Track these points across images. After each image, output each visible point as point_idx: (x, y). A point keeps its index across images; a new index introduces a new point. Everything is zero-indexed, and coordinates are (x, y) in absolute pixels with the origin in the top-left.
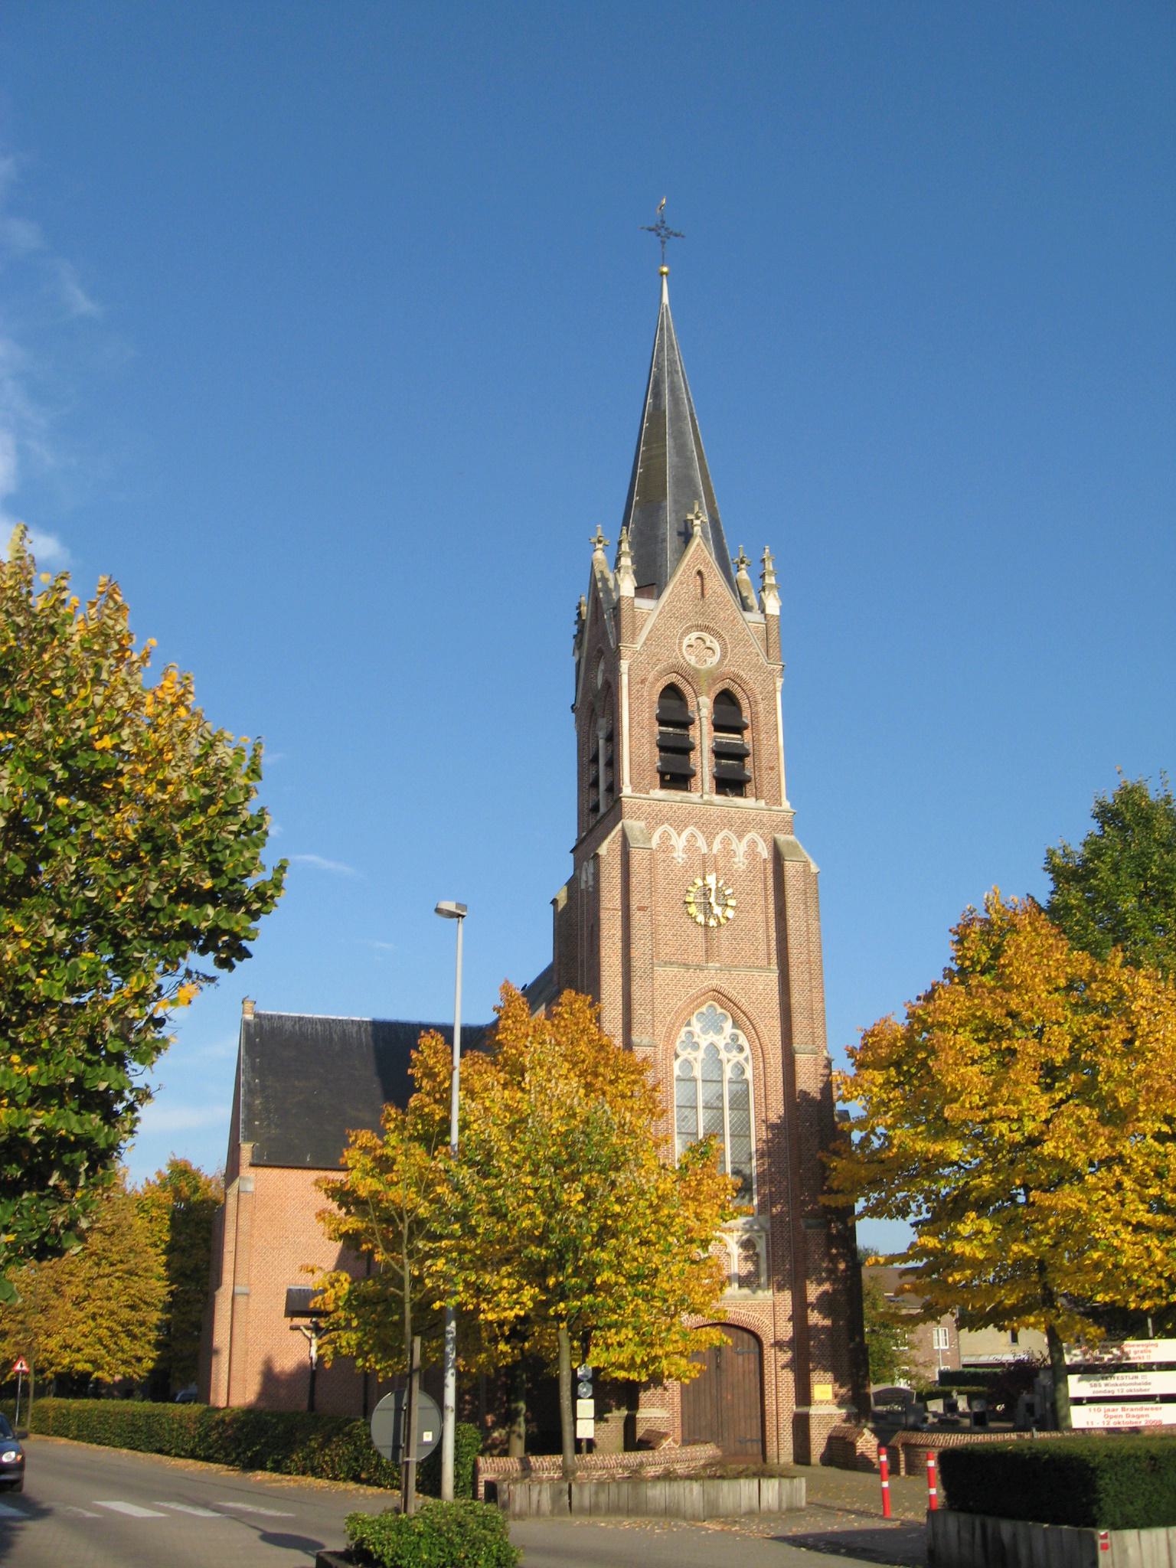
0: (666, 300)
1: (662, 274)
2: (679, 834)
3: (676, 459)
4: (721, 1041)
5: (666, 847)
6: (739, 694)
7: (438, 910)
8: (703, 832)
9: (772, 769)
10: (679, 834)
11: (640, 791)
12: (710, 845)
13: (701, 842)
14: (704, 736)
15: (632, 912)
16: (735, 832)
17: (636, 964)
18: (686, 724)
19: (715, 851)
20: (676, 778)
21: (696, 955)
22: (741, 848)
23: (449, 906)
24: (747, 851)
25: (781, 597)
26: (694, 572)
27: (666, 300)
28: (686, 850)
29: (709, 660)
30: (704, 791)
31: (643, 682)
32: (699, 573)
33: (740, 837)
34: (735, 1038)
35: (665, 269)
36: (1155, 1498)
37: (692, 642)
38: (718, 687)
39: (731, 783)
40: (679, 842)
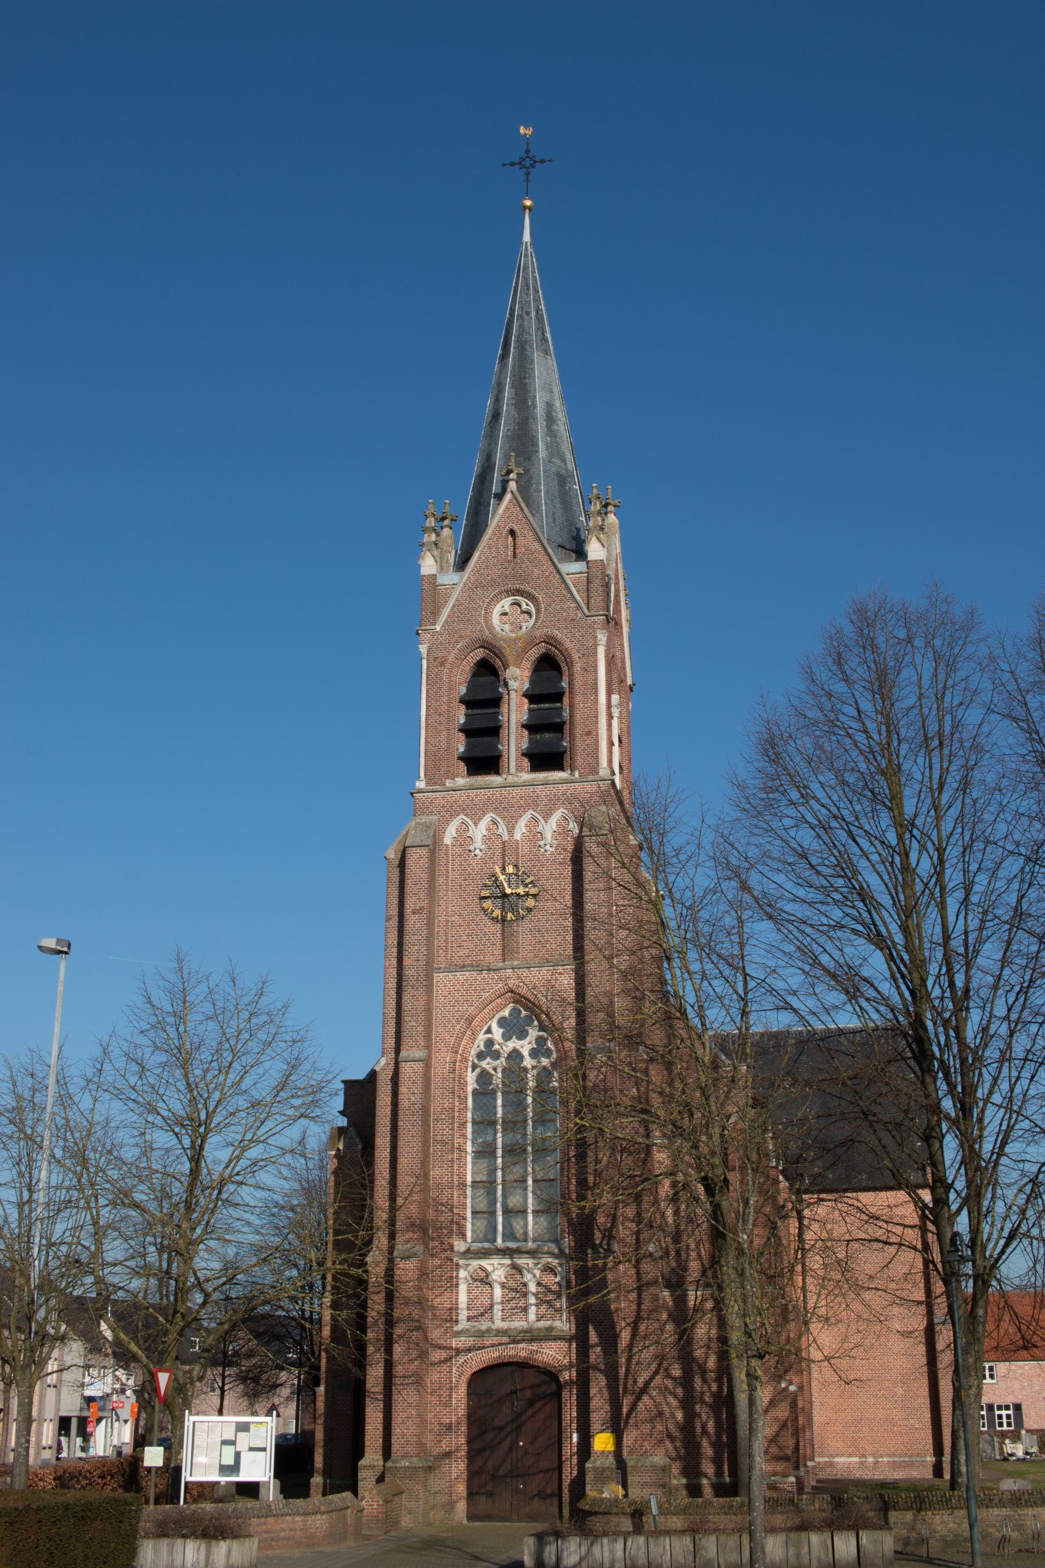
0: (527, 237)
1: (525, 208)
2: (476, 824)
3: (514, 413)
4: (525, 1046)
5: (464, 839)
6: (560, 658)
7: (40, 947)
8: (504, 818)
9: (589, 733)
10: (476, 824)
11: (435, 784)
12: (511, 831)
13: (502, 829)
14: (515, 711)
15: (407, 917)
16: (541, 812)
17: (409, 972)
18: (495, 702)
19: (518, 836)
20: (483, 761)
21: (493, 956)
22: (549, 828)
23: (50, 943)
24: (552, 829)
25: (419, 567)
26: (505, 532)
27: (527, 237)
28: (486, 839)
29: (524, 625)
30: (516, 771)
31: (442, 664)
32: (512, 533)
33: (546, 817)
34: (540, 1041)
35: (528, 203)
36: (84, 1482)
37: (507, 609)
38: (534, 653)
39: (545, 758)
40: (479, 832)
